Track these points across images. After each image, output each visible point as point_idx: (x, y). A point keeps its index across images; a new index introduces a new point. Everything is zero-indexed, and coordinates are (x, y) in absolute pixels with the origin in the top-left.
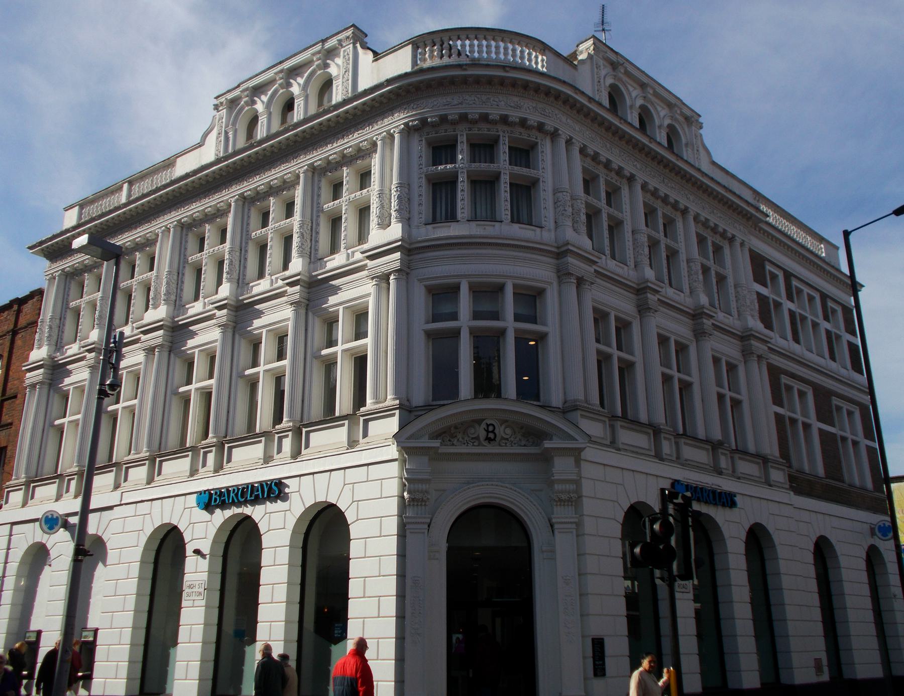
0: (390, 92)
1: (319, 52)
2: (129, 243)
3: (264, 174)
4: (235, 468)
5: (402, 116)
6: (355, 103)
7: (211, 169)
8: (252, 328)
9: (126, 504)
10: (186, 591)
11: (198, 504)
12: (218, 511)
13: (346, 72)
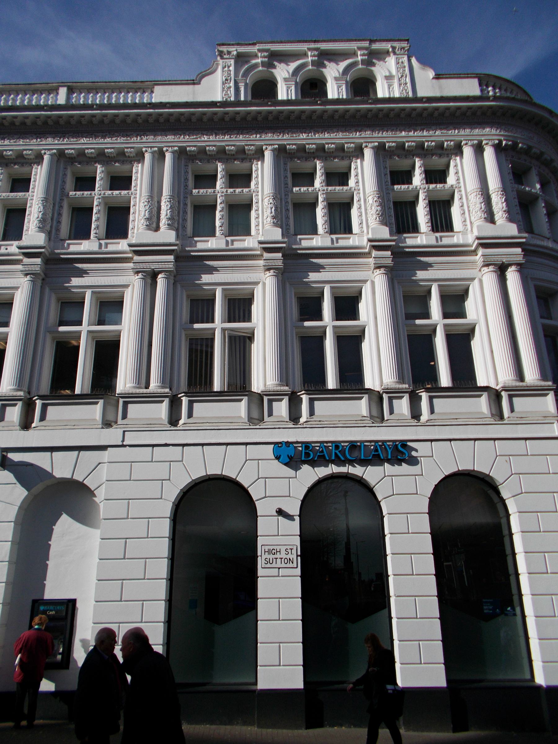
0: (490, 107)
1: (366, 49)
2: (93, 150)
3: (315, 134)
4: (326, 423)
5: (494, 131)
6: (451, 104)
7: (249, 108)
8: (200, 282)
9: (131, 446)
10: (264, 557)
11: (278, 458)
12: (306, 468)
13: (402, 76)
